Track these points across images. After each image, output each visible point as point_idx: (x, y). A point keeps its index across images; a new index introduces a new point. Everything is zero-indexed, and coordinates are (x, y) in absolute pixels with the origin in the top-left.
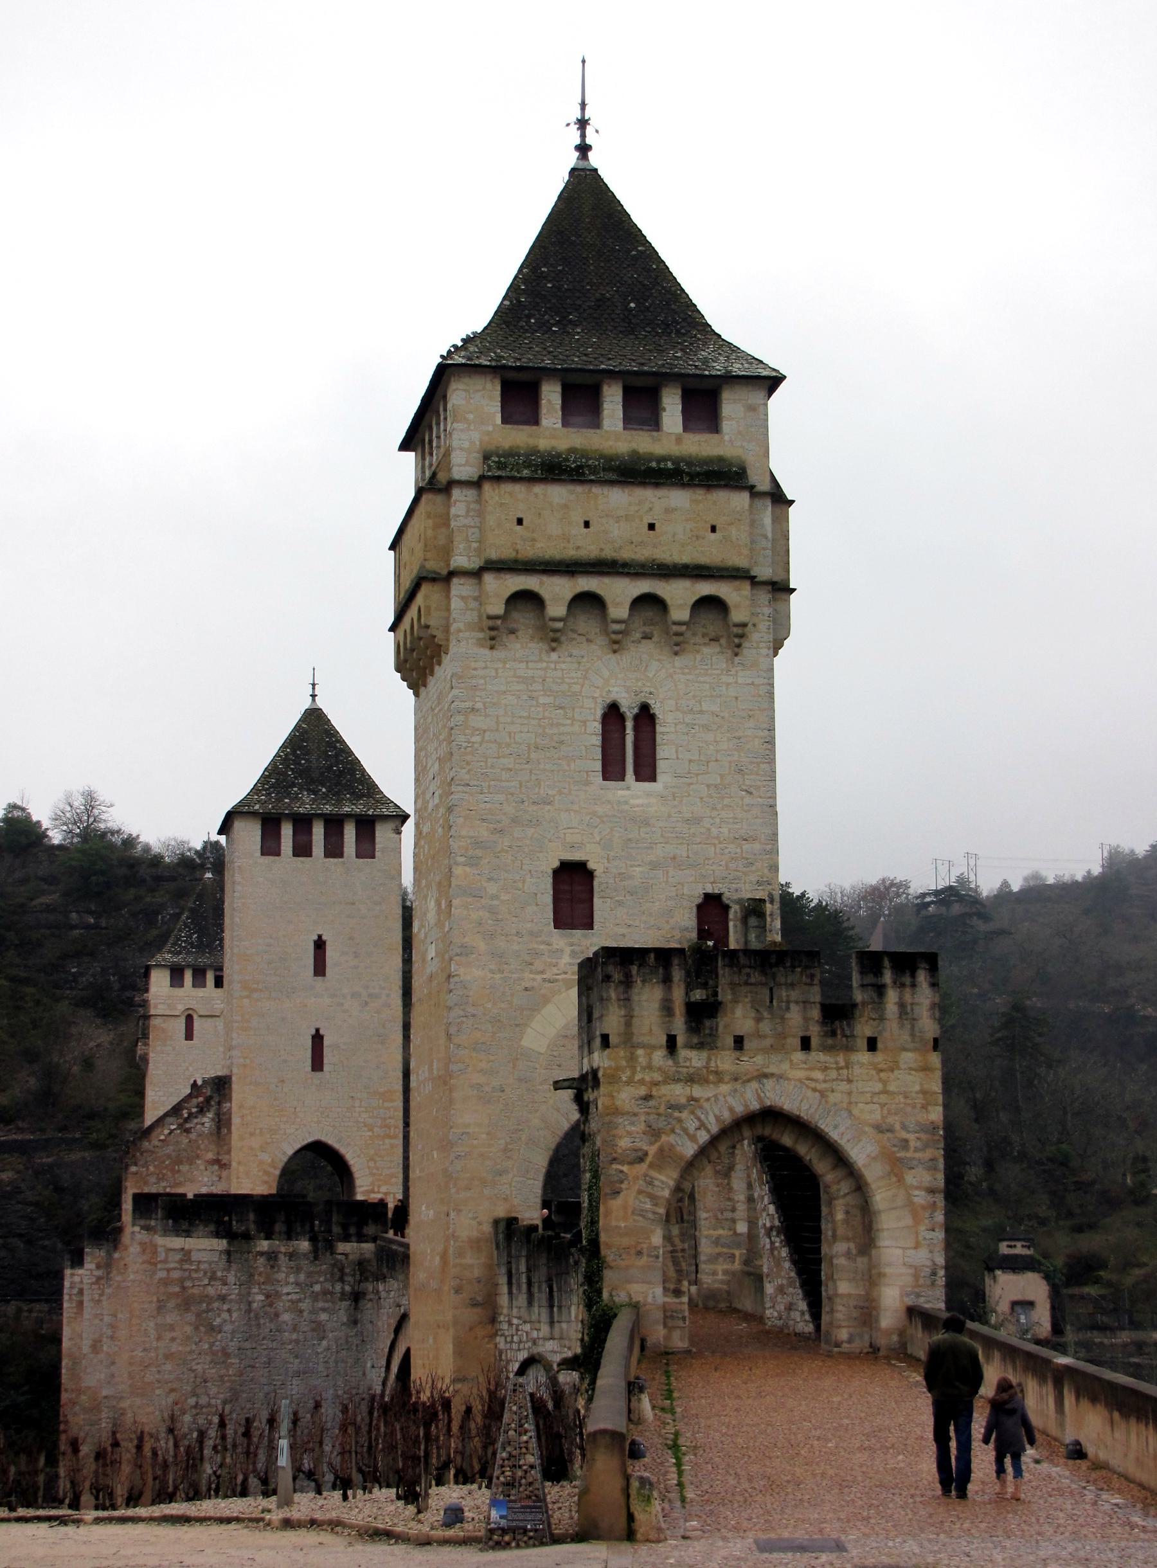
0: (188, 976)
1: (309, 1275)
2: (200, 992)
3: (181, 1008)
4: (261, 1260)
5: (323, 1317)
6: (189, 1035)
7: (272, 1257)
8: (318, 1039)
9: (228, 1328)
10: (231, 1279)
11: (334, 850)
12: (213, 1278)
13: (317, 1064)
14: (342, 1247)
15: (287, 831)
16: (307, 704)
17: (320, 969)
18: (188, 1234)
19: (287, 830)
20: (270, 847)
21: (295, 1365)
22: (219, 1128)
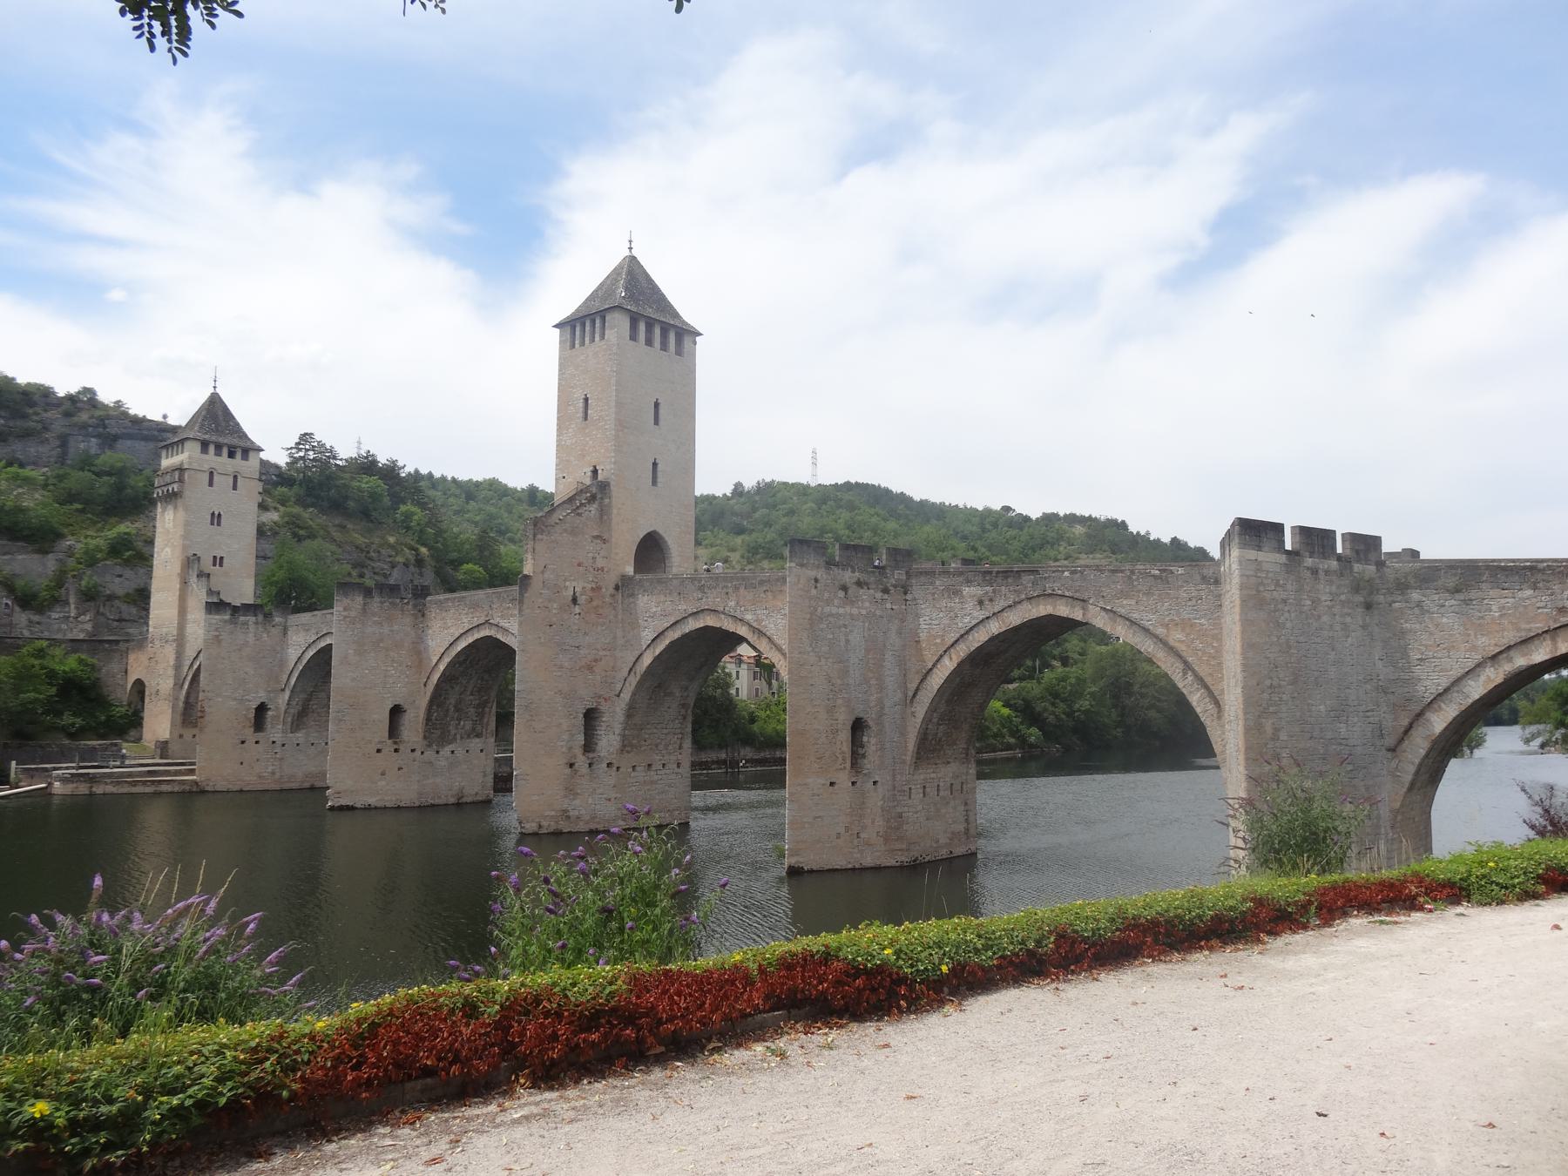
0: (212, 448)
1: (1338, 587)
2: (219, 459)
3: (206, 467)
4: (1308, 574)
5: (1348, 620)
6: (211, 484)
7: (1315, 572)
8: (655, 464)
9: (1289, 625)
10: (1289, 587)
11: (664, 347)
12: (1277, 585)
13: (654, 482)
14: (1357, 567)
15: (642, 327)
16: (627, 253)
17: (656, 422)
18: (1259, 548)
19: (642, 327)
20: (633, 337)
21: (1332, 656)
22: (601, 516)
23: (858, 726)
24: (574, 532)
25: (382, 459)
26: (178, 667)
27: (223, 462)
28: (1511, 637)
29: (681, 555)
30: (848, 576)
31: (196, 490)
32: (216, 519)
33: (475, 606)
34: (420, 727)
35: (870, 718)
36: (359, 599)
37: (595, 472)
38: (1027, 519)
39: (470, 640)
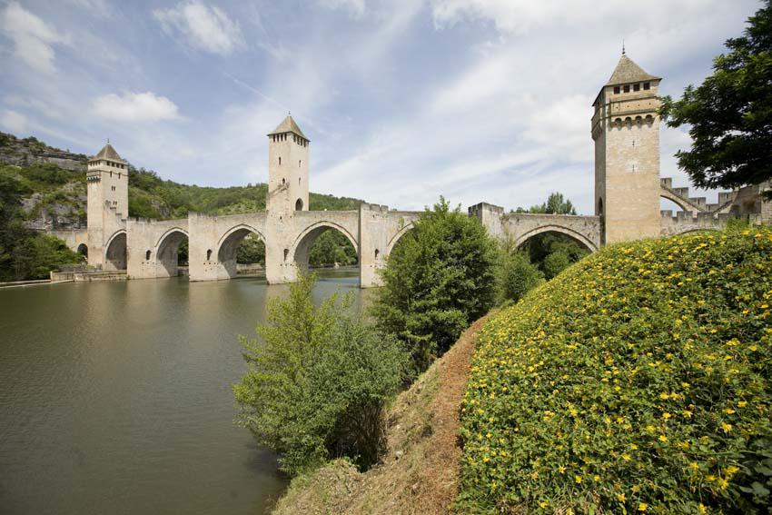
23: (377, 251)
24: (280, 197)
25: (147, 170)
26: (103, 239)
27: (116, 170)
28: (528, 230)
29: (305, 207)
30: (374, 213)
31: (105, 178)
32: (113, 188)
33: (237, 219)
34: (217, 256)
35: (379, 249)
36: (196, 216)
37: (284, 180)
38: (337, 199)
39: (236, 229)
